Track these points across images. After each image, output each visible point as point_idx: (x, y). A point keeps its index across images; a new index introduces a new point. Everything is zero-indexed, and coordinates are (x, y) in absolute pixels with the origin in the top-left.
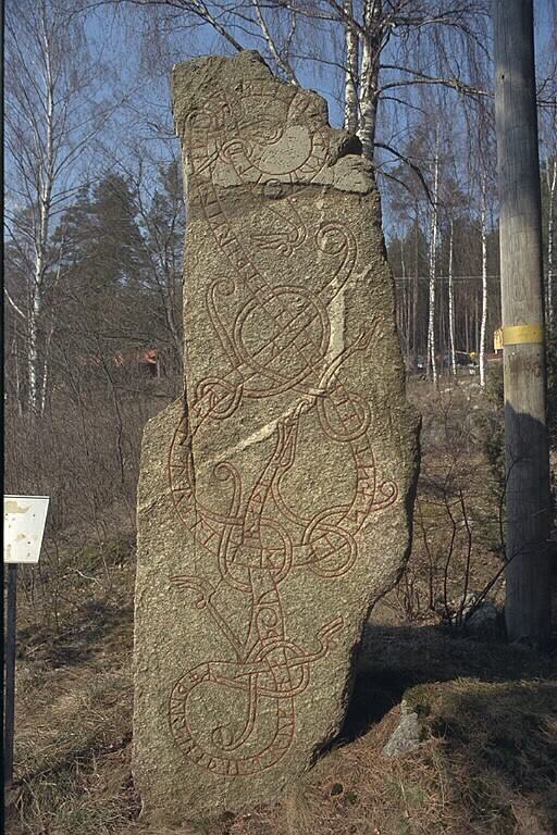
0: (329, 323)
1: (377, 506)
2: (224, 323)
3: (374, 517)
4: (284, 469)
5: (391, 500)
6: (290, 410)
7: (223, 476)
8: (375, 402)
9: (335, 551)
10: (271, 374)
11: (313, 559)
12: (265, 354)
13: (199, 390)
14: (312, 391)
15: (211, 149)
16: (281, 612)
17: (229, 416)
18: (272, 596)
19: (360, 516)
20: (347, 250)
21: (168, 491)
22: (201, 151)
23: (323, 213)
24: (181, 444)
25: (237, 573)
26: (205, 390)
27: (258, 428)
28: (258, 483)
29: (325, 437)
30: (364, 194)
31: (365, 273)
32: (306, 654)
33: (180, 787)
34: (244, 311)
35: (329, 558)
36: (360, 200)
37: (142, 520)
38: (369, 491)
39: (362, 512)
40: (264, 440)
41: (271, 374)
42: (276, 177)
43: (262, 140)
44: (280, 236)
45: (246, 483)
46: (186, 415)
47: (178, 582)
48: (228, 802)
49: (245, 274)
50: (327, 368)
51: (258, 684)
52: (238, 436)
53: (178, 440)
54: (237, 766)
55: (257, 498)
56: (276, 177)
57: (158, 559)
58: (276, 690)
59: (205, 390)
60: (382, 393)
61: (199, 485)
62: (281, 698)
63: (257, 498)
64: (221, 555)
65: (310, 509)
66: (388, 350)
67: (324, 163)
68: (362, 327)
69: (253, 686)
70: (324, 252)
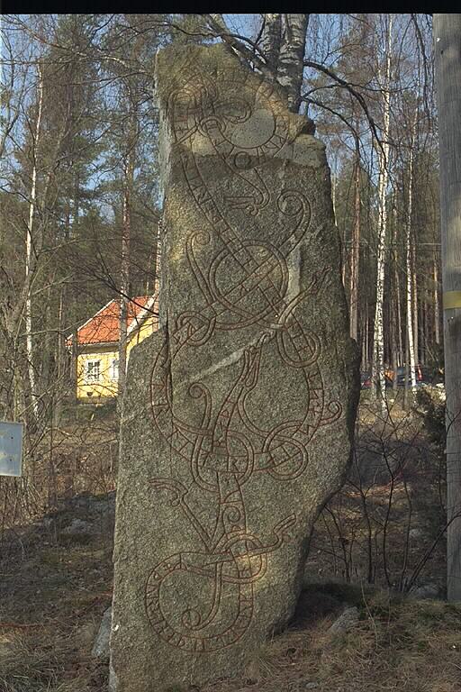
0: (288, 271)
2: (201, 267)
3: (323, 430)
5: (336, 417)
6: (255, 341)
7: (196, 395)
11: (272, 463)
12: (234, 294)
13: (179, 322)
14: (272, 325)
16: (243, 509)
17: (204, 344)
20: (303, 213)
21: (149, 405)
22: (183, 125)
25: (207, 476)
27: (228, 354)
28: (226, 400)
29: (283, 364)
30: (317, 169)
32: (265, 545)
33: (153, 663)
34: (218, 258)
35: (285, 463)
38: (318, 409)
39: (312, 427)
43: (233, 119)
45: (216, 399)
46: (166, 342)
47: (155, 484)
48: (194, 677)
49: (219, 228)
50: (285, 308)
51: (223, 572)
52: (210, 361)
54: (203, 643)
55: (225, 414)
57: (138, 463)
58: (239, 577)
59: (184, 321)
60: (329, 329)
61: (176, 401)
62: (243, 583)
63: (225, 414)
64: (193, 460)
66: (335, 295)
68: (314, 275)
69: (218, 574)
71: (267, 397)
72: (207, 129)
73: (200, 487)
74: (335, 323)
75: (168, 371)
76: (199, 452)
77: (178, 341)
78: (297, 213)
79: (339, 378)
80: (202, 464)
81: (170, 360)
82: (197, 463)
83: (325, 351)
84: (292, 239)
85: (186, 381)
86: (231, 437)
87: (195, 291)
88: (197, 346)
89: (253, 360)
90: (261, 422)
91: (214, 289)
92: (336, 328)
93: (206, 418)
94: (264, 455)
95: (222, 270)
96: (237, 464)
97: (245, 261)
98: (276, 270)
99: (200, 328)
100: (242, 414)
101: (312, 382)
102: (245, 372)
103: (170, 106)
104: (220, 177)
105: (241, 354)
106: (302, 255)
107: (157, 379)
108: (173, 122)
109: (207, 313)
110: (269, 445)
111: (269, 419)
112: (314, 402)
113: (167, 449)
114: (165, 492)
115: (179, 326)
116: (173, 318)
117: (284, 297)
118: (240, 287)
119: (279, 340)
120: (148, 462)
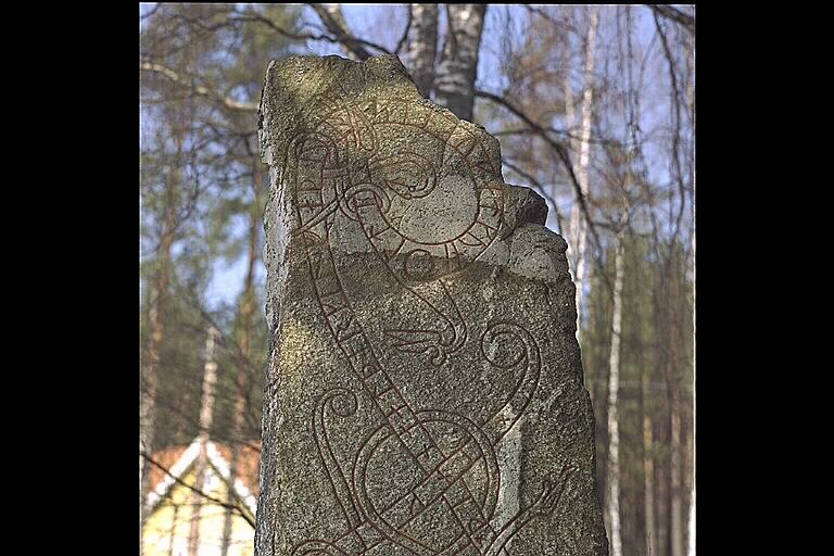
0: (498, 470)
2: (338, 458)
10: (406, 543)
15: (328, 195)
20: (526, 365)
23: (491, 306)
31: (552, 399)
34: (371, 442)
36: (547, 292)
41: (406, 543)
42: (423, 247)
44: (428, 336)
49: (374, 386)
50: (493, 539)
56: (423, 247)
67: (495, 234)
70: (492, 364)
72: (357, 208)
78: (515, 364)
84: (507, 411)
87: (328, 502)
91: (362, 501)
95: (379, 465)
97: (420, 447)
98: (476, 466)
103: (291, 161)
104: (378, 293)
106: (524, 440)
108: (295, 192)
118: (409, 497)
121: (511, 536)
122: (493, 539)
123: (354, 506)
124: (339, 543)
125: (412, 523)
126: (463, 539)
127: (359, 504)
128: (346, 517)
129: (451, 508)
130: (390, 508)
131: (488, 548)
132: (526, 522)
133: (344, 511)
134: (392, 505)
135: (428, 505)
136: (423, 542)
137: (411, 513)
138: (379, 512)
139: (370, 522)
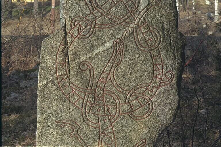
1: (163, 84)
3: (162, 89)
4: (116, 65)
5: (170, 81)
6: (120, 36)
7: (84, 69)
8: (163, 33)
9: (142, 106)
12: (107, 6)
13: (72, 24)
14: (131, 25)
17: (88, 37)
18: (110, 129)
19: (155, 89)
21: (55, 76)
24: (62, 52)
26: (76, 23)
27: (103, 43)
29: (138, 49)
35: (139, 109)
37: (40, 91)
38: (159, 77)
39: (156, 87)
40: (106, 50)
41: (110, 17)
45: (97, 71)
46: (65, 36)
47: (60, 123)
50: (139, 14)
52: (92, 48)
53: (61, 49)
55: (102, 80)
57: (49, 111)
59: (76, 23)
60: (166, 27)
61: (72, 73)
63: (102, 80)
64: (84, 108)
65: (130, 85)
66: (170, 5)
71: (128, 70)
73: (87, 124)
74: (169, 23)
75: (67, 55)
76: (86, 104)
77: (72, 36)
79: (172, 57)
80: (88, 111)
81: (68, 48)
82: (85, 110)
83: (163, 41)
85: (78, 60)
86: (106, 94)
88: (84, 39)
89: (119, 47)
90: (124, 85)
91: (94, 3)
92: (170, 26)
93: (91, 83)
94: (126, 105)
96: (110, 110)
99: (86, 28)
100: (112, 80)
101: (155, 60)
102: (114, 54)
105: (111, 43)
107: (60, 59)
109: (90, 18)
110: (129, 99)
111: (129, 83)
112: (157, 73)
113: (67, 102)
114: (66, 128)
115: (73, 26)
116: (69, 21)
117: (138, 7)
119: (135, 34)
120: (56, 110)
121: (145, 13)
122: (139, 14)
123: (92, 5)
124: (87, 18)
125: (111, 10)
126: (129, 14)
127: (93, 4)
128: (89, 8)
129: (125, 4)
130: (104, 5)
131: (137, 17)
132: (150, 8)
133: (88, 6)
134: (105, 4)
135: (117, 3)
136: (115, 16)
137: (111, 6)
138: (100, 6)
139: (97, 10)
